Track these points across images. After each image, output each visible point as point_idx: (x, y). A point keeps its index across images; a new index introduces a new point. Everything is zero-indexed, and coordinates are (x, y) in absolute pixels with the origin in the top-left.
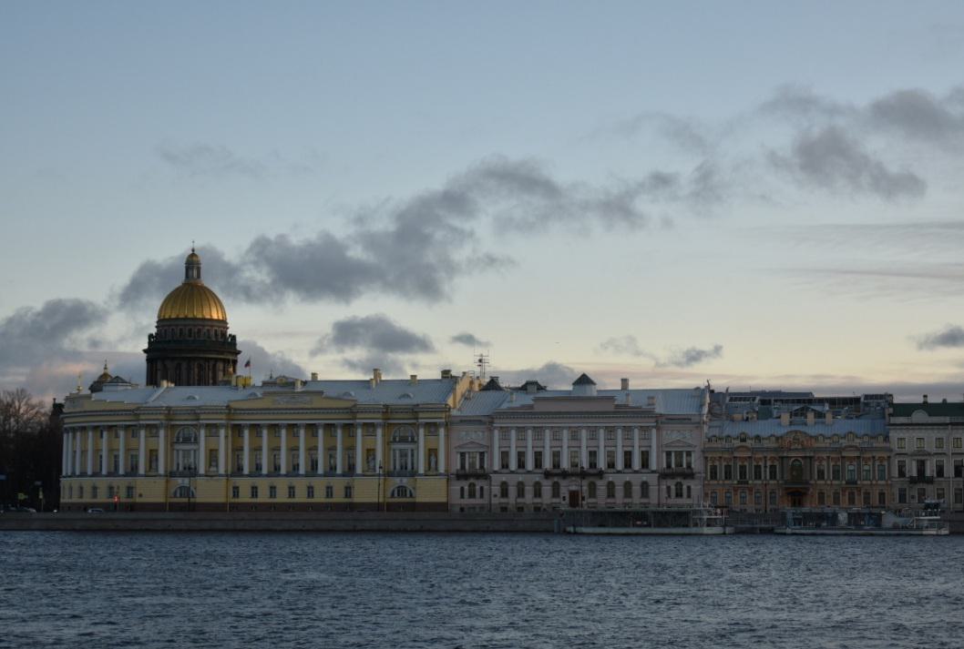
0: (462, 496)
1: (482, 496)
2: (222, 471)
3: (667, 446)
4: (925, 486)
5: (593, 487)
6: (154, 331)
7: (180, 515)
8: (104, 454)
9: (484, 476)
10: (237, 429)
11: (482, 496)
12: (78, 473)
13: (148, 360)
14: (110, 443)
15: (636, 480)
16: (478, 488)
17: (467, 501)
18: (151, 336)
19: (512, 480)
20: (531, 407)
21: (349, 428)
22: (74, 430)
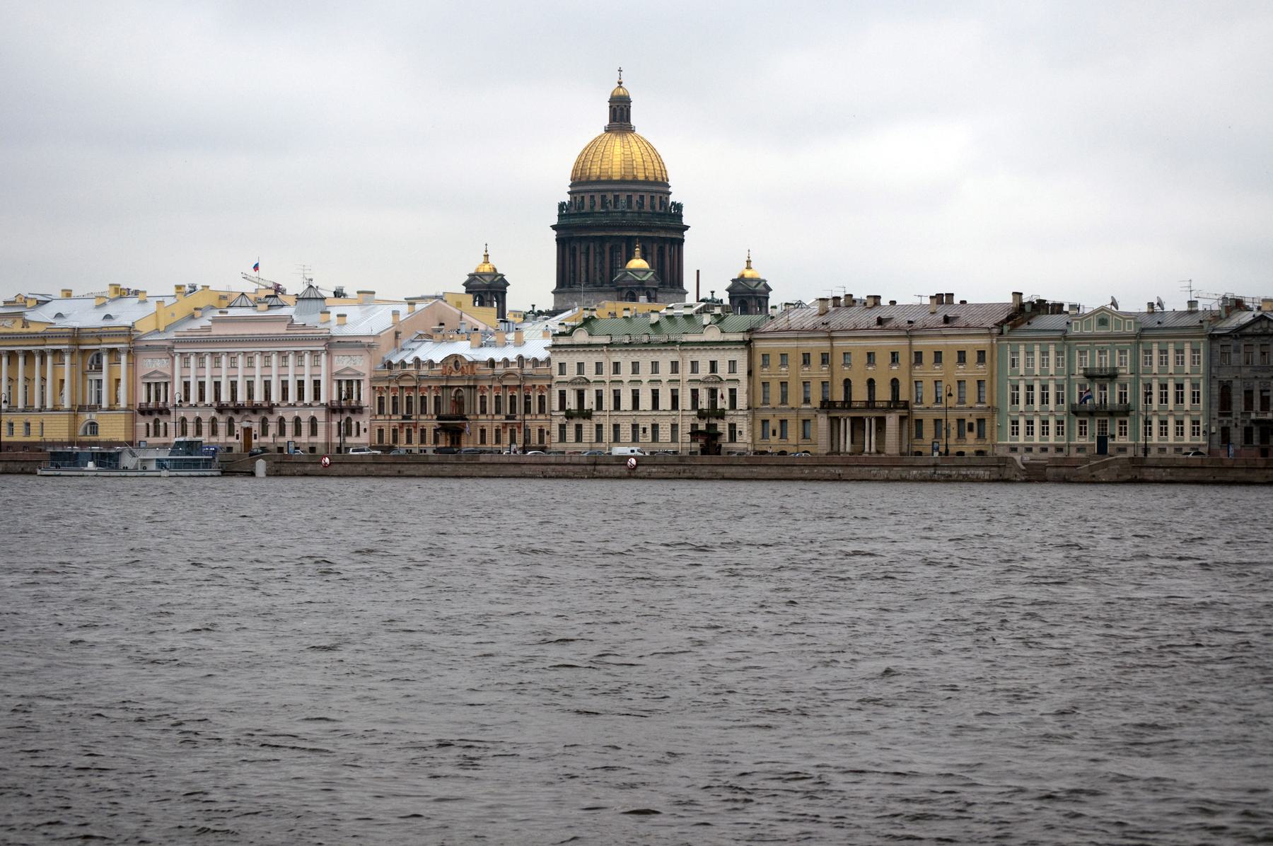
1: (166, 435)
3: (337, 374)
4: (581, 421)
5: (264, 423)
6: (567, 198)
9: (164, 411)
11: (166, 435)
12: (49, 405)
13: (559, 241)
16: (161, 424)
18: (562, 206)
20: (209, 329)
21: (43, 355)
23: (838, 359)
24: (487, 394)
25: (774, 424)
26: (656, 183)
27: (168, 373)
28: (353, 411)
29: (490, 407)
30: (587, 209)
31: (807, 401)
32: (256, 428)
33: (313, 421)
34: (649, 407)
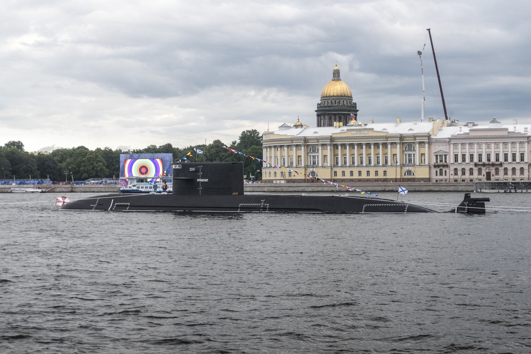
0: (437, 175)
1: (446, 175)
2: (329, 165)
6: (320, 102)
7: (309, 184)
8: (279, 158)
9: (447, 166)
10: (336, 146)
13: (318, 115)
14: (275, 153)
16: (444, 171)
17: (439, 177)
20: (468, 134)
21: (385, 145)
22: (266, 147)
26: (348, 97)
27: (447, 151)
30: (326, 104)
32: (493, 172)
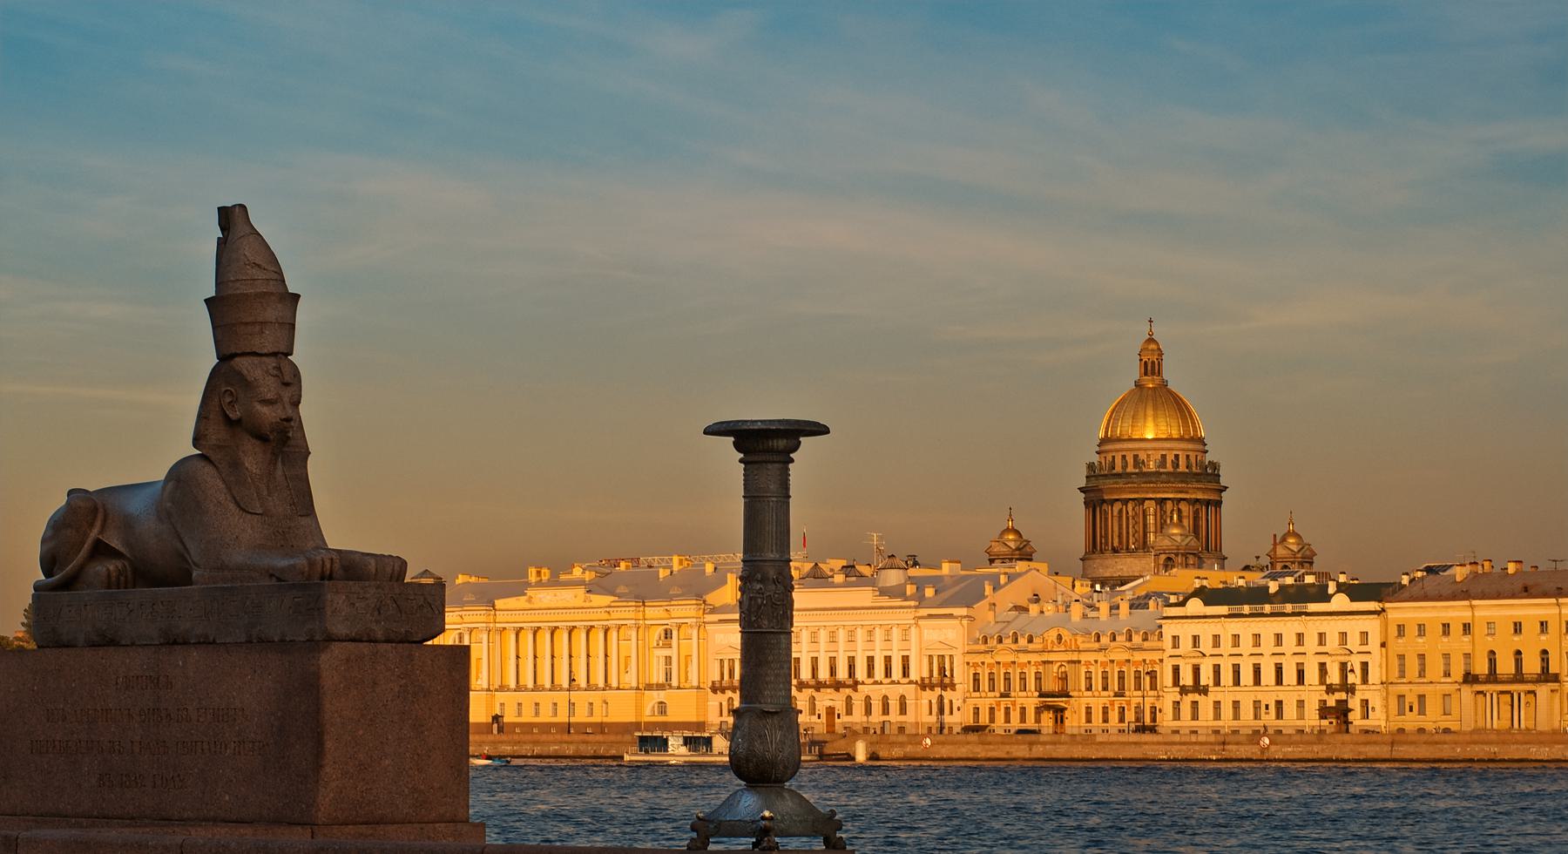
4: (1196, 697)
15: (894, 693)
19: (876, 693)
23: (1479, 630)
24: (1092, 669)
25: (1411, 699)
28: (944, 687)
29: (1097, 682)
31: (1447, 674)
32: (840, 706)
33: (903, 698)
34: (1273, 682)
